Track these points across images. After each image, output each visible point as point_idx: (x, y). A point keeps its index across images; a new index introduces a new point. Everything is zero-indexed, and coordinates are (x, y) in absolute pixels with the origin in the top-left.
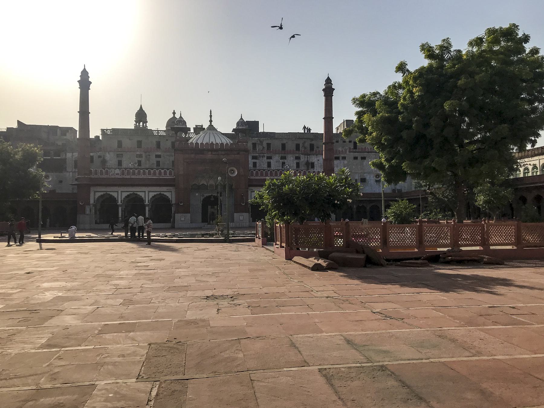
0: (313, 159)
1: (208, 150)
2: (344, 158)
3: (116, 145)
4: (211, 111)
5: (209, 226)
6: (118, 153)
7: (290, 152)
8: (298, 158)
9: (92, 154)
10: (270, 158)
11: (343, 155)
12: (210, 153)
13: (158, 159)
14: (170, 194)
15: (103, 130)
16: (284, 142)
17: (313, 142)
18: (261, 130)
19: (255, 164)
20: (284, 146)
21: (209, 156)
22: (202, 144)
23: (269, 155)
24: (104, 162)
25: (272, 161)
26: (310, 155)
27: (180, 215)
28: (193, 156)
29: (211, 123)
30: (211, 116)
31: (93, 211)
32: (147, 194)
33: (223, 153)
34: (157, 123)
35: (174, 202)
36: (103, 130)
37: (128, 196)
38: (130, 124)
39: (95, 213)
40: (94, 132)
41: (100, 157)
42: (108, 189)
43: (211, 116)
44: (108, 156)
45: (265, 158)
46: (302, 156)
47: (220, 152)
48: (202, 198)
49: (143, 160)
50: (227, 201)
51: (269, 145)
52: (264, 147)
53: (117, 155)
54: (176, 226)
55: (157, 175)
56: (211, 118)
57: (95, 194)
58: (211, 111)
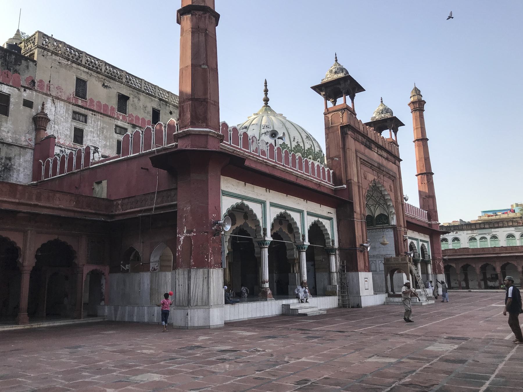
3: (71, 88)
4: (266, 83)
6: (77, 109)
24: (40, 121)
29: (266, 104)
30: (266, 91)
41: (28, 104)
43: (266, 91)
44: (50, 110)
53: (75, 113)
56: (266, 94)
58: (266, 83)
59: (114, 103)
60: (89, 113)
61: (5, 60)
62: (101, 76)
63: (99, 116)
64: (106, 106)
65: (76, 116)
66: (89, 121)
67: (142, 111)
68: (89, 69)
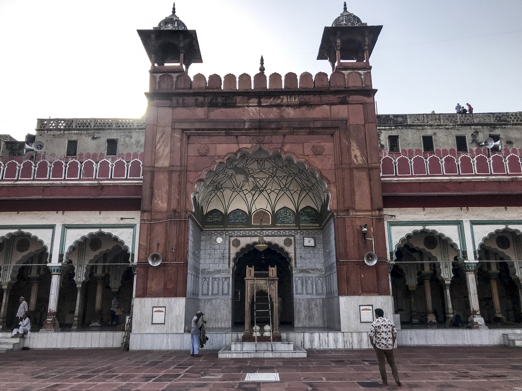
1: (248, 94)
5: (248, 346)
12: (254, 101)
15: (41, 122)
16: (429, 132)
21: (252, 112)
27: (149, 302)
33: (295, 100)
36: (41, 122)
47: (285, 100)
48: (234, 251)
50: (309, 260)
51: (393, 140)
59: (104, 149)
61: (12, 149)
62: (90, 132)
67: (134, 147)
68: (78, 130)
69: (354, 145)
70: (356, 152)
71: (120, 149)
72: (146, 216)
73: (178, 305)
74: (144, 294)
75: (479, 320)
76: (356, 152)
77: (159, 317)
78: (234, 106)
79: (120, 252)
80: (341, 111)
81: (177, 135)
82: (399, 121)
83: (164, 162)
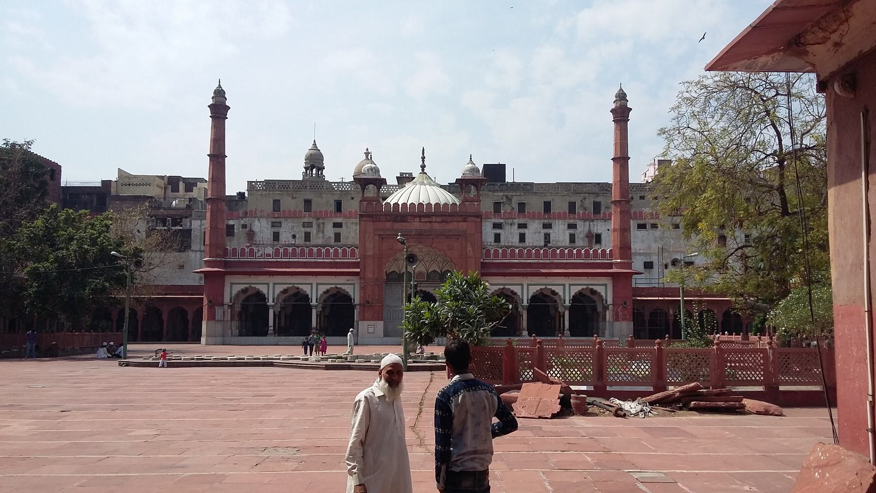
0: (599, 227)
2: (654, 226)
3: (270, 207)
6: (274, 220)
7: (560, 217)
8: (572, 226)
9: (231, 222)
10: (523, 226)
11: (652, 221)
12: (417, 219)
13: (337, 230)
14: (353, 289)
15: (250, 183)
16: (548, 199)
17: (598, 199)
18: (509, 179)
19: (497, 238)
20: (547, 206)
21: (416, 225)
22: (404, 205)
23: (522, 221)
24: (251, 235)
25: (526, 231)
26: (593, 221)
27: (366, 323)
28: (388, 224)
29: (423, 170)
30: (423, 158)
31: (228, 316)
32: (315, 289)
33: (439, 219)
34: (339, 171)
35: (357, 301)
36: (250, 183)
37: (285, 291)
38: (295, 172)
39: (232, 319)
40: (234, 186)
41: (244, 226)
42: (253, 279)
43: (423, 158)
45: (516, 226)
46: (579, 224)
47: (434, 219)
49: (313, 231)
52: (513, 209)
53: (273, 223)
54: (360, 341)
55: (332, 255)
56: (423, 161)
57: (233, 287)
59: (301, 206)
60: (282, 220)
63: (289, 220)
64: (295, 212)
65: (273, 225)
66: (283, 225)
69: (469, 246)
70: (470, 248)
71: (314, 207)
72: (362, 281)
73: (380, 324)
74: (363, 319)
75: (525, 333)
76: (470, 248)
77: (371, 330)
78: (407, 222)
79: (347, 298)
80: (463, 225)
81: (377, 238)
82: (527, 188)
83: (370, 253)
